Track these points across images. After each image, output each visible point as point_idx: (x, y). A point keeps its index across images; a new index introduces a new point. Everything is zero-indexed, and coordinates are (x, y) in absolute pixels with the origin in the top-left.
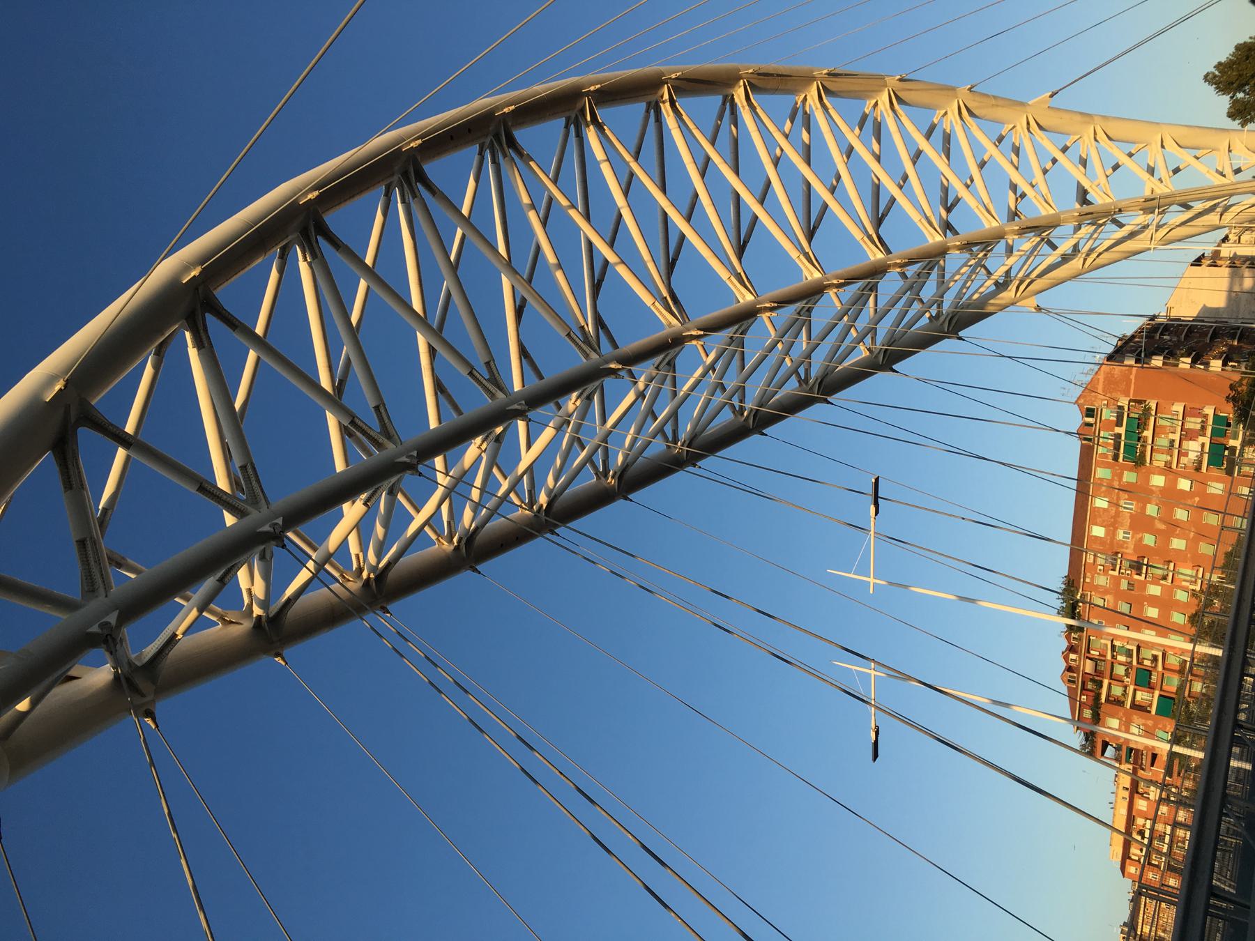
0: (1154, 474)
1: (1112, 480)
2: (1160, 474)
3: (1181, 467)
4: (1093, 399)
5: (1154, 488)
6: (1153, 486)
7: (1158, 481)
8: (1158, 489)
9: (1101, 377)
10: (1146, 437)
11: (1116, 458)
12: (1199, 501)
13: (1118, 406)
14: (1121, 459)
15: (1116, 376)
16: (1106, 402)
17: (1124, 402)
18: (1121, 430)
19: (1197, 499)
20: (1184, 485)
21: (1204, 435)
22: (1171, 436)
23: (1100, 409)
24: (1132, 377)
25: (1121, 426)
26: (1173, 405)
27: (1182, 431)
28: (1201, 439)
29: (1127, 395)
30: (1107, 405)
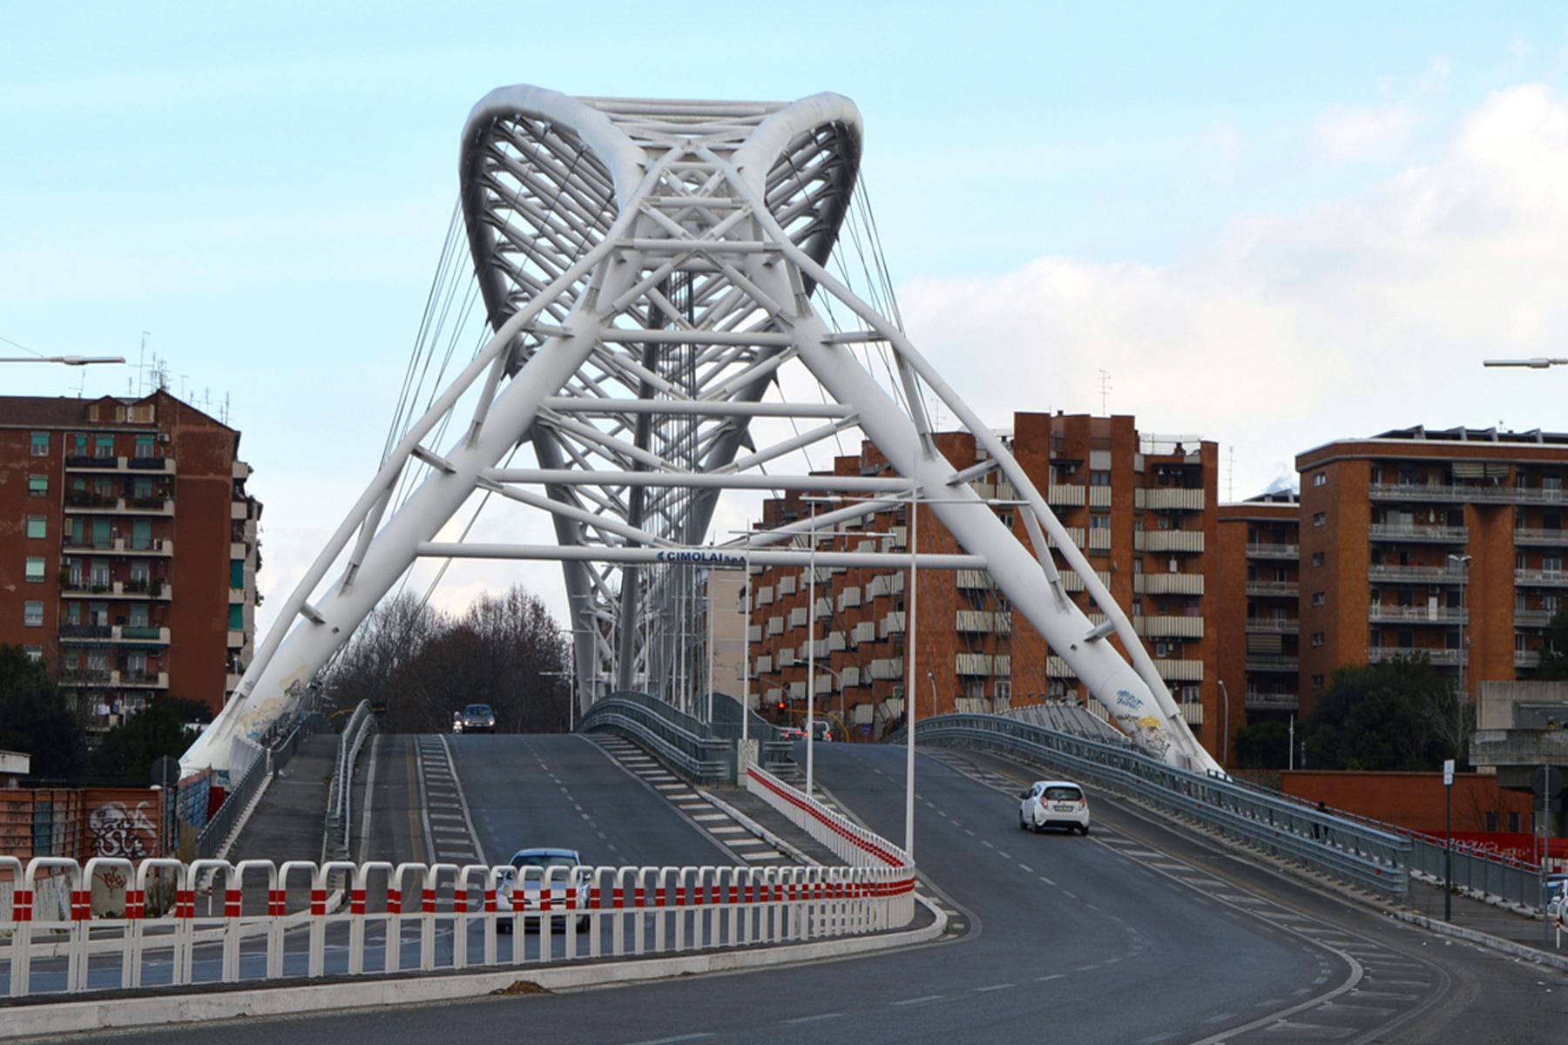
0: (47, 522)
1: (30, 458)
2: (48, 529)
3: (65, 561)
4: (170, 419)
5: (23, 522)
6: (27, 521)
7: (37, 529)
8: (22, 529)
9: (208, 428)
10: (112, 503)
11: (70, 463)
12: (8, 591)
13: (162, 461)
14: (68, 470)
15: (211, 451)
16: (167, 439)
17: (170, 466)
18: (123, 466)
19: (12, 588)
20: (35, 569)
21: (125, 590)
22: (120, 543)
23: (154, 430)
24: (211, 476)
25: (130, 466)
26: (172, 540)
27: (128, 557)
28: (118, 586)
29: (179, 470)
30: (163, 443)
